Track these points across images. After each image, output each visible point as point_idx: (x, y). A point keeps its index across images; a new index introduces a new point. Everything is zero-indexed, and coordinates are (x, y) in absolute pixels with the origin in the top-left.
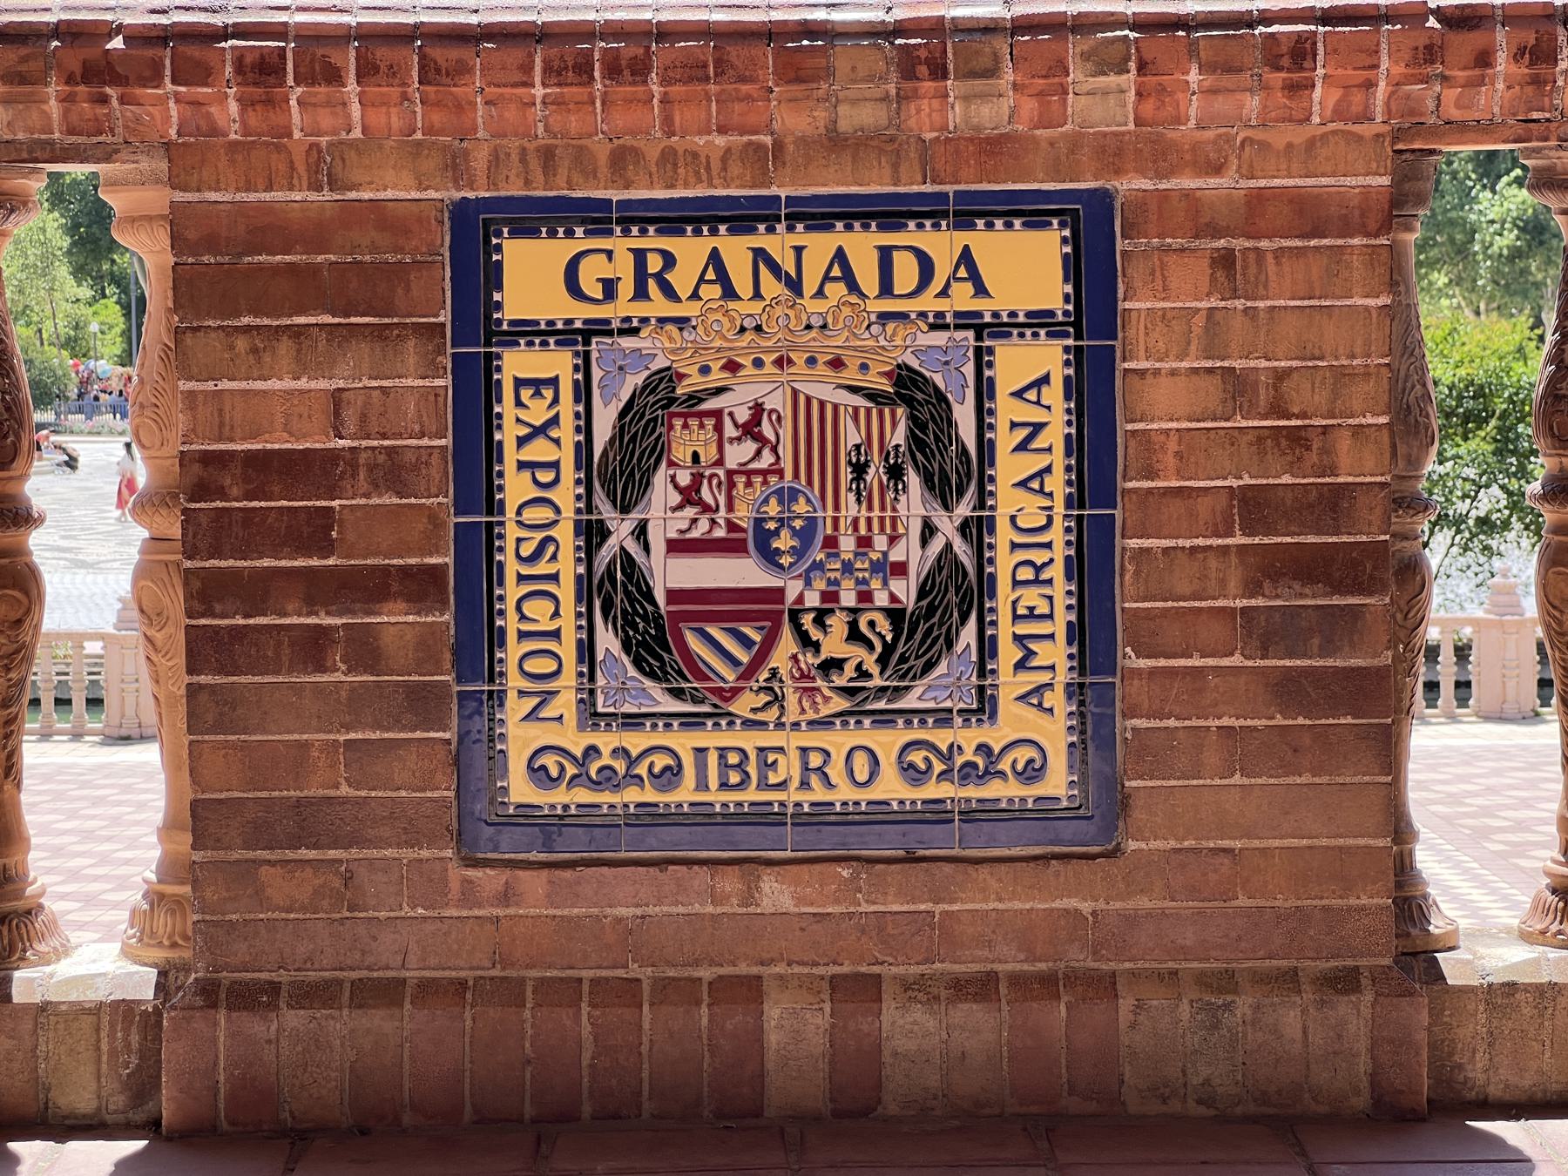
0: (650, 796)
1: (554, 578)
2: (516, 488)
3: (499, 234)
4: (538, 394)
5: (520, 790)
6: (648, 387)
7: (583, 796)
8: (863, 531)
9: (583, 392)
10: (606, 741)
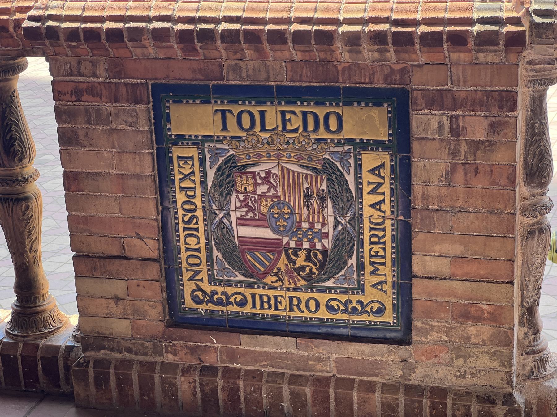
0: (235, 308)
1: (197, 230)
2: (181, 198)
3: (168, 101)
4: (186, 163)
5: (189, 303)
6: (226, 162)
7: (211, 307)
8: (311, 221)
9: (202, 162)
10: (220, 289)
